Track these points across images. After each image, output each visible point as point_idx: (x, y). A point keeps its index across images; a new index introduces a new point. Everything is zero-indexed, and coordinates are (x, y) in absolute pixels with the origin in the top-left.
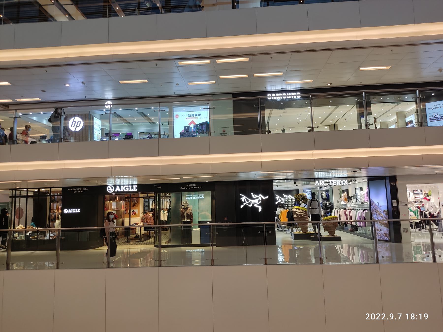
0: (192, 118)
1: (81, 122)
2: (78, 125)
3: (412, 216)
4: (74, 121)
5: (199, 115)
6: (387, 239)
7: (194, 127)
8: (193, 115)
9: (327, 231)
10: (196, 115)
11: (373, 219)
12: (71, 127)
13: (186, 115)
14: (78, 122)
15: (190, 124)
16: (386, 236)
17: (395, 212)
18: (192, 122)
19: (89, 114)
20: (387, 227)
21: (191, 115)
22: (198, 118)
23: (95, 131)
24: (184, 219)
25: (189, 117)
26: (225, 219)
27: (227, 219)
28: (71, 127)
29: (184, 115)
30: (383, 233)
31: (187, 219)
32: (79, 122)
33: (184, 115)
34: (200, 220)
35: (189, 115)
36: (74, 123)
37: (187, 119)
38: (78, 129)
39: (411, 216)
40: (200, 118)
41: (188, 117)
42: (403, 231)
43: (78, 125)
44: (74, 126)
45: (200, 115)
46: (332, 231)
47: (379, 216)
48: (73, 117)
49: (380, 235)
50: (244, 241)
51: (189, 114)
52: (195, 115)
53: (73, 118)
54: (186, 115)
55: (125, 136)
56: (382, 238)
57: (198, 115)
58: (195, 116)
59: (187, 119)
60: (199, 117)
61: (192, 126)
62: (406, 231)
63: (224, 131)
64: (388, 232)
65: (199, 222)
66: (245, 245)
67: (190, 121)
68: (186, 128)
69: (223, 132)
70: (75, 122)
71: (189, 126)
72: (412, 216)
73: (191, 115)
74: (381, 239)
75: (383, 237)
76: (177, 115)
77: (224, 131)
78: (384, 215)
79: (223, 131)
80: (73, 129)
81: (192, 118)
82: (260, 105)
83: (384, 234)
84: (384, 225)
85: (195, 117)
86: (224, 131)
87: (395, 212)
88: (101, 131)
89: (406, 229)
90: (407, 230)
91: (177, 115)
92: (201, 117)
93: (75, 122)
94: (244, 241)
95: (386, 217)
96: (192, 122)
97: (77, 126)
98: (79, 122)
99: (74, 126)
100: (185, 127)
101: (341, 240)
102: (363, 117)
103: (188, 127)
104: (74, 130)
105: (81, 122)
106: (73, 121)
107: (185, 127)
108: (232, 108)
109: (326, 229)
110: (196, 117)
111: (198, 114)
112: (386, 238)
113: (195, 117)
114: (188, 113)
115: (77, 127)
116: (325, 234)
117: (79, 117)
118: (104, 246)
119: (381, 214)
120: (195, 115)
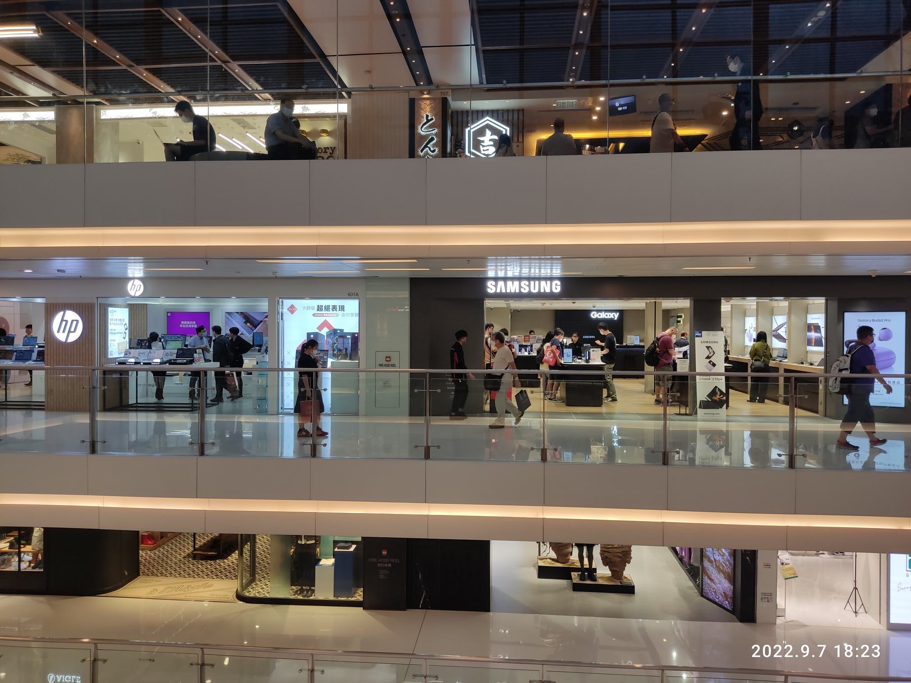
0: (324, 315)
1: (77, 321)
2: (72, 330)
3: (786, 564)
4: (65, 319)
5: (340, 308)
6: (726, 604)
7: (328, 335)
8: (327, 308)
9: (608, 567)
10: (334, 308)
11: (705, 553)
12: (58, 332)
13: (313, 308)
14: (72, 321)
15: (321, 327)
16: (727, 600)
17: (748, 558)
18: (325, 324)
19: (95, 304)
20: (730, 582)
21: (324, 308)
22: (337, 315)
23: (110, 337)
24: (301, 540)
25: (318, 312)
26: (384, 553)
27: (387, 552)
28: (58, 332)
29: (308, 308)
30: (721, 589)
31: (307, 541)
32: (75, 323)
33: (308, 308)
34: (337, 538)
35: (319, 308)
36: (64, 323)
37: (314, 315)
38: (73, 337)
39: (783, 564)
40: (343, 315)
41: (315, 311)
42: (760, 599)
43: (72, 330)
44: (64, 332)
45: (342, 308)
46: (618, 570)
47: (717, 553)
48: (62, 310)
49: (715, 592)
50: (422, 600)
51: (318, 306)
52: (331, 307)
53: (62, 313)
54: (313, 308)
55: (178, 349)
56: (718, 599)
57: (338, 309)
58: (331, 311)
59: (314, 315)
60: (340, 313)
61: (325, 331)
62: (767, 598)
63: (387, 359)
64: (731, 592)
65: (336, 543)
66: (425, 607)
67: (320, 320)
68: (312, 336)
69: (386, 361)
70: (67, 321)
71: (317, 331)
72: (786, 564)
73: (324, 308)
74: (717, 600)
75: (721, 598)
76: (292, 306)
77: (388, 358)
78: (727, 555)
79: (387, 359)
80: (61, 337)
81: (324, 315)
82: (426, 392)
83: (723, 593)
84: (724, 574)
85: (331, 312)
86: (388, 358)
87: (748, 558)
88: (127, 332)
89: (768, 595)
90: (771, 597)
91: (292, 306)
92: (344, 312)
93: (67, 321)
94: (422, 600)
95: (729, 560)
96: (325, 324)
97: (69, 332)
98: (75, 323)
99: (64, 332)
100: (309, 334)
101: (634, 593)
102: (700, 334)
103: (316, 334)
104: (63, 340)
105: (77, 321)
106: (62, 320)
107: (309, 334)
108: (407, 309)
109: (606, 561)
110: (335, 312)
111: (338, 307)
112: (727, 602)
113: (331, 312)
114: (316, 303)
115: (71, 334)
116: (603, 571)
117: (74, 310)
118: (139, 575)
119: (722, 551)
120: (331, 307)
